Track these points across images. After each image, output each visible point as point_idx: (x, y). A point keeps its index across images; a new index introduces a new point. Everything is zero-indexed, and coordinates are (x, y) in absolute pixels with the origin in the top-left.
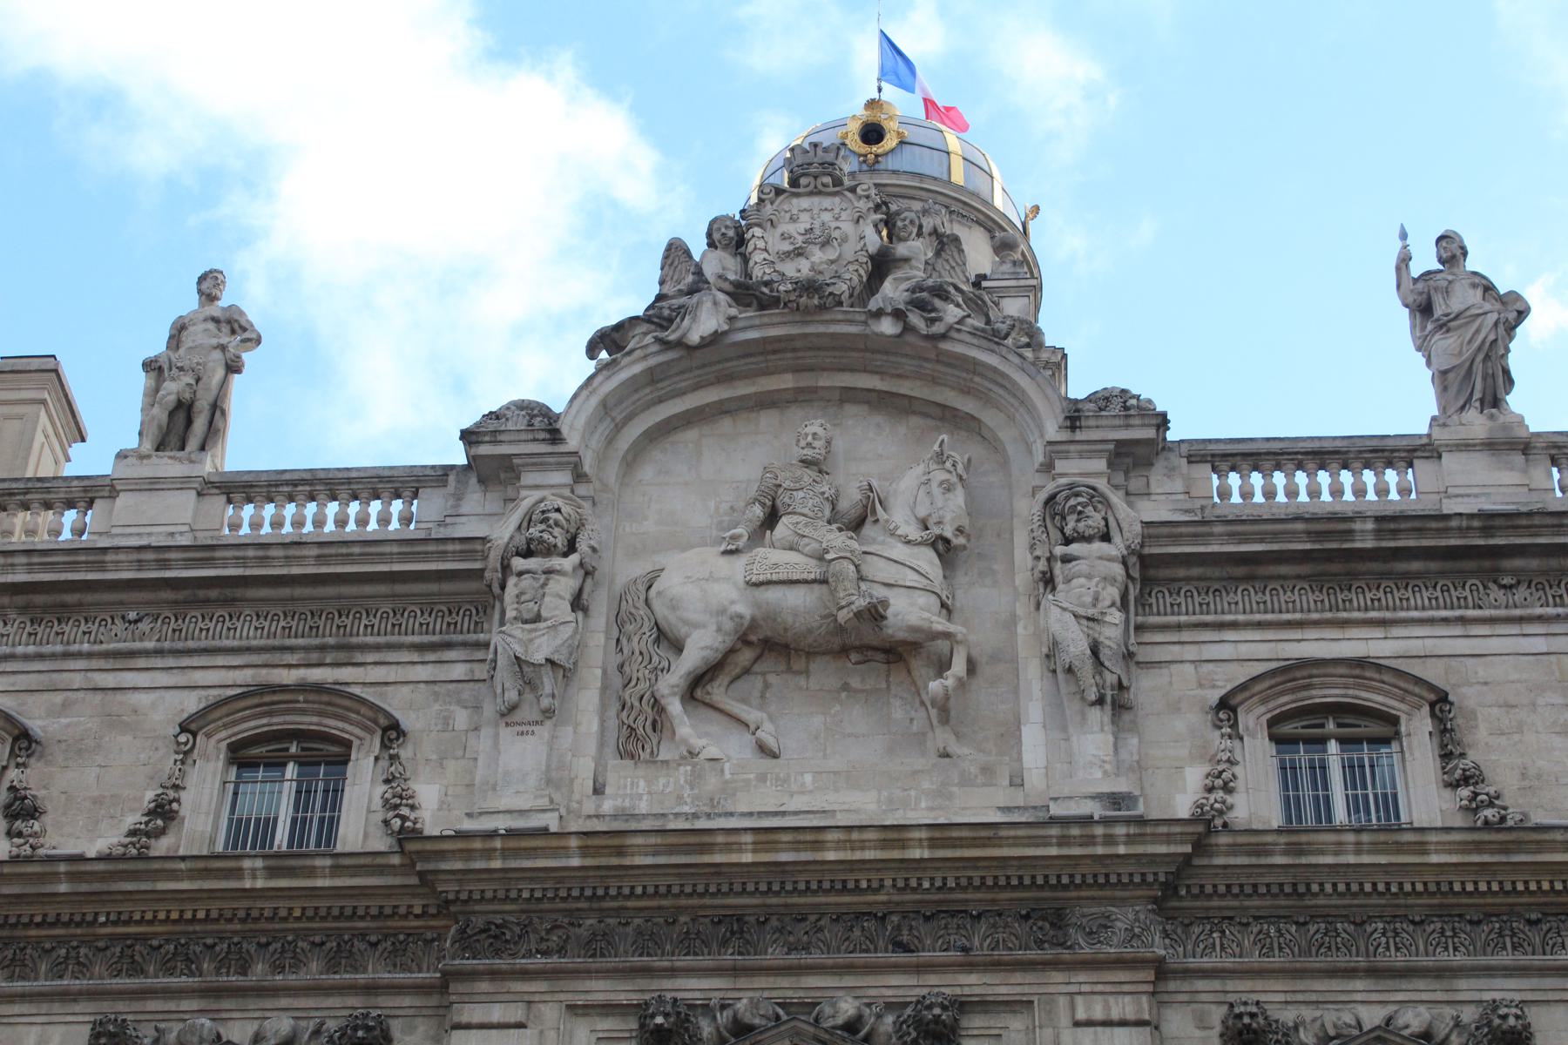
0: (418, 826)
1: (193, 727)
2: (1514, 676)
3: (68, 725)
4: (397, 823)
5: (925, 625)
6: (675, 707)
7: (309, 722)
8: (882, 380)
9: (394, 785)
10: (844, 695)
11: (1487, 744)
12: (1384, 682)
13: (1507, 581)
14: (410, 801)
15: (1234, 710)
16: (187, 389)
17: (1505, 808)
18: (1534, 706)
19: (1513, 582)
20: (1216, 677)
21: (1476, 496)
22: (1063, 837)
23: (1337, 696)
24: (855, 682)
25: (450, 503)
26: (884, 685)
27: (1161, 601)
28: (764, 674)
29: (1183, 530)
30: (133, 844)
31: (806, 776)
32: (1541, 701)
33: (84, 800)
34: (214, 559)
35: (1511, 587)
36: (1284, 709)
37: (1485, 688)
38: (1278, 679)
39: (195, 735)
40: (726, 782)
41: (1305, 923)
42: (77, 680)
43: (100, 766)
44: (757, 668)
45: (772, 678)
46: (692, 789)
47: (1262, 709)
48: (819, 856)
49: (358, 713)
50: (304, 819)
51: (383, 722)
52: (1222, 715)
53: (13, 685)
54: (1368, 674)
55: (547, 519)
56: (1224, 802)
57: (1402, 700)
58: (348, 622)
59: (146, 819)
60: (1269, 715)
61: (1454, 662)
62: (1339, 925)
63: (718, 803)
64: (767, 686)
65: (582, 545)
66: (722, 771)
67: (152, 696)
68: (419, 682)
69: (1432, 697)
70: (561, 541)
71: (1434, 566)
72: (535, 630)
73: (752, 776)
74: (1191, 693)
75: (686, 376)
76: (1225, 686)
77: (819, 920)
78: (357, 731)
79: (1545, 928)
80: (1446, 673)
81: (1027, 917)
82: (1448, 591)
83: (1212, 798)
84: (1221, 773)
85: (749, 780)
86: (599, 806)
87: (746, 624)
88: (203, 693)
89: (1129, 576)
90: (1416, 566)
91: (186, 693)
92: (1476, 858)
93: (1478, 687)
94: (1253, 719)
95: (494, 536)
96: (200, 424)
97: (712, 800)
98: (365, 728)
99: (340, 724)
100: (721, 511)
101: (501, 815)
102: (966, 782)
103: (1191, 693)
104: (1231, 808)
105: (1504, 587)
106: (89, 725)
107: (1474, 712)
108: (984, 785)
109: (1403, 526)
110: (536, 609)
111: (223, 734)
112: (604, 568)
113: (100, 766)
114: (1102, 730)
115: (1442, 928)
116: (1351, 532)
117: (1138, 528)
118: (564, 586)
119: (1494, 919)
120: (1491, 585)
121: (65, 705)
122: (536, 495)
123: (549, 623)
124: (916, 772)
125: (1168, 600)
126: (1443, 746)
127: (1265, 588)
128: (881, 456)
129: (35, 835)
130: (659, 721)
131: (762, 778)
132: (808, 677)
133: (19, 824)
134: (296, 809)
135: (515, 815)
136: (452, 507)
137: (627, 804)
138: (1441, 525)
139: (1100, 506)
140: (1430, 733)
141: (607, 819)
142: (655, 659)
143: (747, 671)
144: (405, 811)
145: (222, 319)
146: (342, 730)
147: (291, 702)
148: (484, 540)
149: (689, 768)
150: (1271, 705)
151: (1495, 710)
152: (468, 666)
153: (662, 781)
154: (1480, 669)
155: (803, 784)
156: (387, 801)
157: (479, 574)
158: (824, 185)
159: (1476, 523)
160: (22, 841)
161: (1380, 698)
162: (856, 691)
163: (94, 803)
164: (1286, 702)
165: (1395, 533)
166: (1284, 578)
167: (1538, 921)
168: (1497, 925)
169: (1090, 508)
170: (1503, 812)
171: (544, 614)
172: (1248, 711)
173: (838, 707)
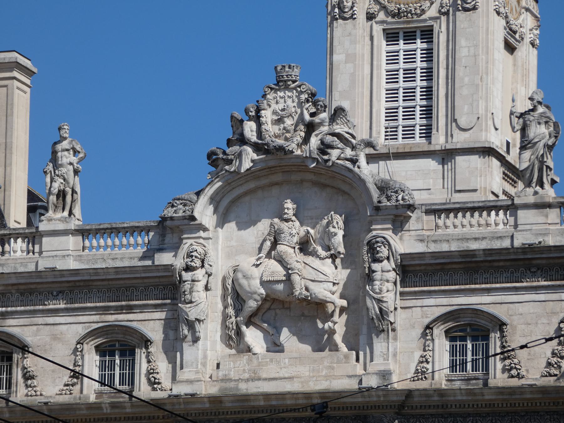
0: (160, 381)
1: (81, 342)
2: (532, 311)
3: (40, 340)
4: (153, 379)
5: (325, 299)
6: (244, 328)
7: (120, 337)
8: (315, 175)
9: (150, 364)
10: (302, 318)
11: (518, 341)
12: (484, 316)
13: (533, 270)
14: (157, 371)
15: (432, 329)
16: (61, 185)
17: (520, 369)
18: (537, 323)
19: (535, 270)
20: (428, 313)
21: (526, 230)
22: (362, 395)
23: (469, 321)
24: (306, 313)
25: (161, 239)
26: (316, 314)
27: (410, 279)
28: (275, 309)
29: (415, 256)
30: (67, 389)
31: (286, 359)
32: (539, 322)
33: (49, 371)
34: (79, 274)
35: (535, 272)
36: (450, 326)
37: (521, 316)
38: (447, 316)
39: (82, 344)
40: (260, 362)
41: (447, 417)
42: (40, 320)
43: (52, 356)
44: (272, 307)
45: (278, 311)
46: (248, 366)
47: (442, 327)
48: (285, 402)
49: (136, 334)
50: (123, 373)
51: (145, 339)
52: (428, 331)
53: (19, 322)
54: (479, 313)
55: (192, 256)
56: (425, 368)
57: (491, 323)
58: (129, 294)
59: (70, 379)
60: (445, 329)
61: (511, 305)
62: (458, 419)
63: (257, 372)
64: (276, 314)
65: (206, 265)
66: (258, 358)
67: (67, 326)
68: (156, 320)
69: (500, 323)
70: (198, 263)
71: (508, 264)
72: (190, 307)
73: (268, 360)
74: (418, 320)
75: (241, 179)
76: (430, 317)
77: (289, 420)
78: (137, 341)
79: (526, 418)
80: (508, 310)
81: (355, 419)
82: (513, 273)
83: (422, 365)
84: (425, 356)
85: (267, 362)
86: (218, 374)
87: (264, 296)
88: (83, 325)
89: (397, 274)
90: (501, 264)
91: (78, 325)
92: (501, 397)
93: (518, 316)
94: (439, 331)
95: (175, 264)
96: (69, 198)
97: (255, 371)
98: (139, 340)
99: (131, 338)
100: (259, 235)
101: (184, 383)
102: (339, 362)
103: (418, 320)
104: (427, 370)
105: (532, 272)
106: (47, 339)
107: (516, 327)
108: (345, 363)
109: (493, 252)
110: (190, 298)
111: (92, 342)
112: (213, 270)
113: (52, 356)
114: (384, 341)
115: (492, 419)
116: (475, 255)
117: (399, 257)
118: (200, 286)
119: (510, 414)
120: (528, 272)
121: (38, 330)
122: (190, 242)
123: (195, 304)
124: (322, 358)
125: (413, 279)
126: (502, 343)
127: (448, 273)
128: (316, 207)
129: (35, 386)
130: (239, 333)
131: (271, 360)
132: (290, 311)
133: (29, 382)
134: (120, 370)
135: (189, 383)
136: (162, 241)
137: (227, 373)
138: (507, 251)
139: (386, 246)
140: (499, 338)
141: (220, 382)
142: (237, 306)
143: (269, 309)
144: (155, 375)
145: (69, 148)
146: (132, 340)
147: (113, 330)
148: (172, 265)
149: (247, 357)
150: (446, 325)
151: (523, 326)
152: (172, 312)
153: (239, 362)
154: (520, 308)
155: (285, 363)
156: (148, 371)
157: (173, 276)
158: (289, 85)
159: (520, 251)
160: (31, 389)
161: (483, 322)
162: (307, 316)
163: (53, 372)
164: (450, 325)
165: (491, 255)
166: (455, 269)
167: (524, 415)
168: (510, 417)
169: (383, 247)
170: (519, 371)
171: (193, 300)
172: (438, 327)
173: (300, 323)
